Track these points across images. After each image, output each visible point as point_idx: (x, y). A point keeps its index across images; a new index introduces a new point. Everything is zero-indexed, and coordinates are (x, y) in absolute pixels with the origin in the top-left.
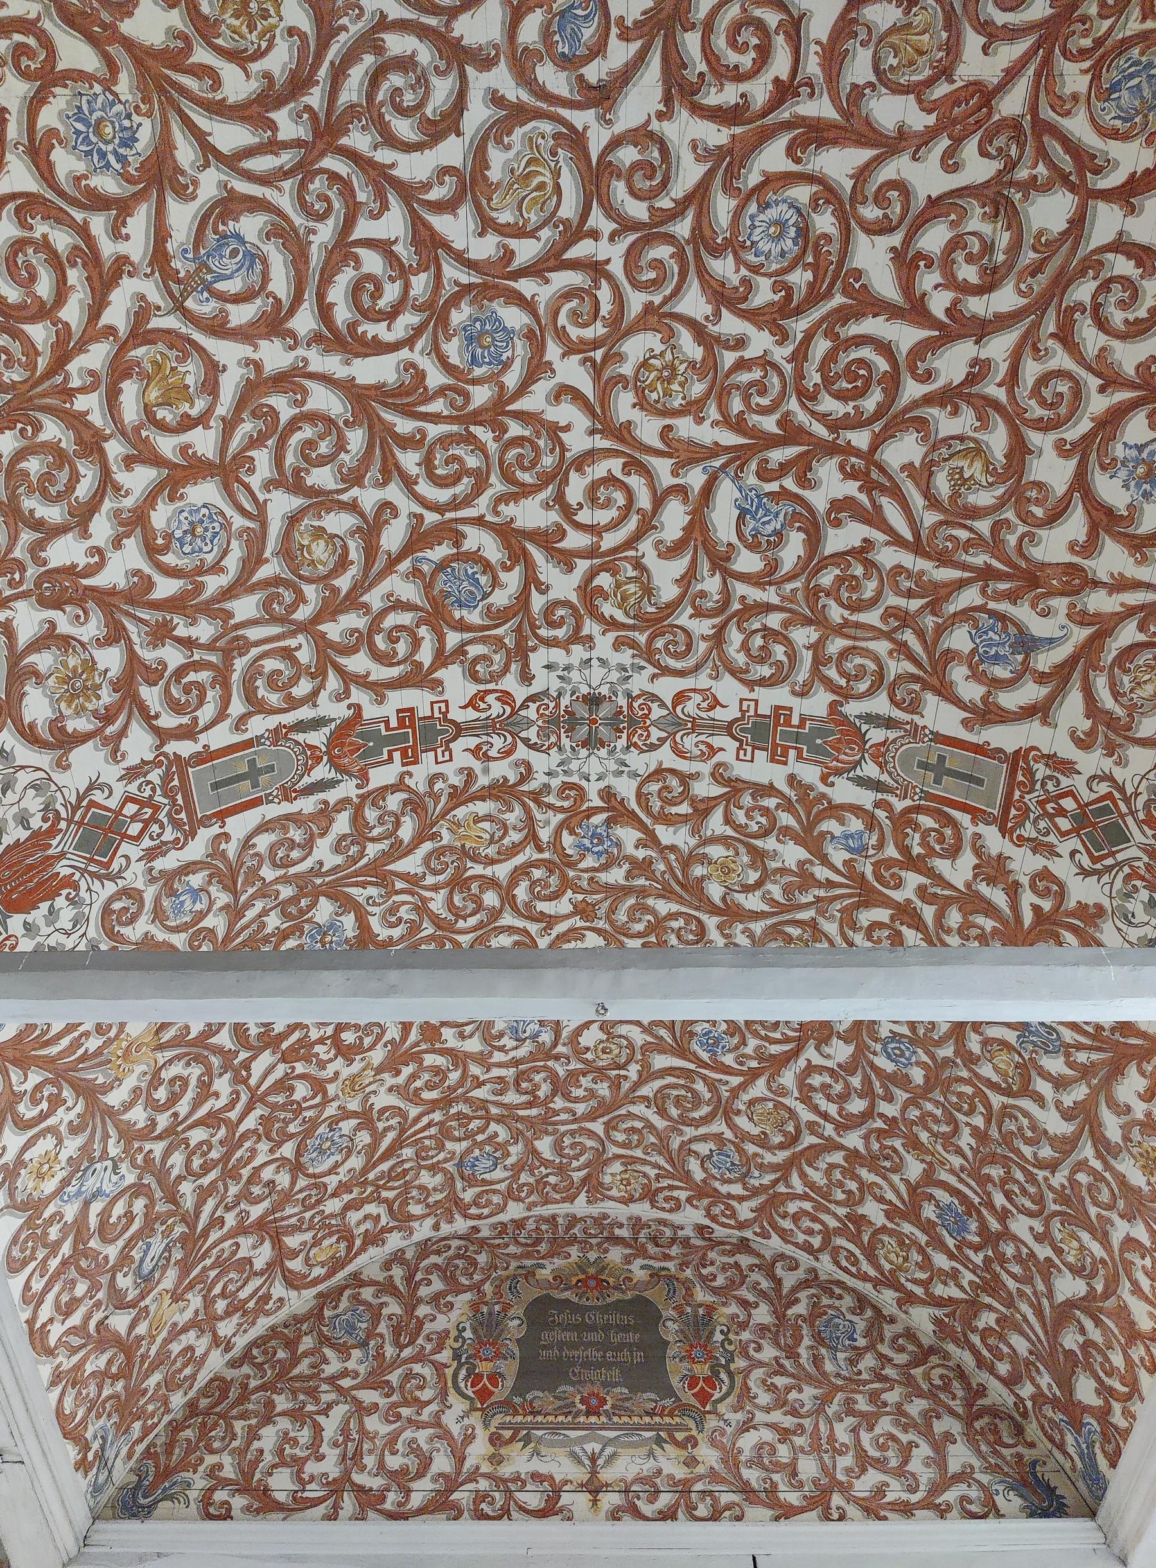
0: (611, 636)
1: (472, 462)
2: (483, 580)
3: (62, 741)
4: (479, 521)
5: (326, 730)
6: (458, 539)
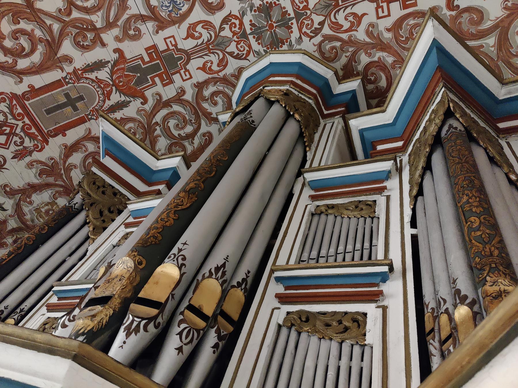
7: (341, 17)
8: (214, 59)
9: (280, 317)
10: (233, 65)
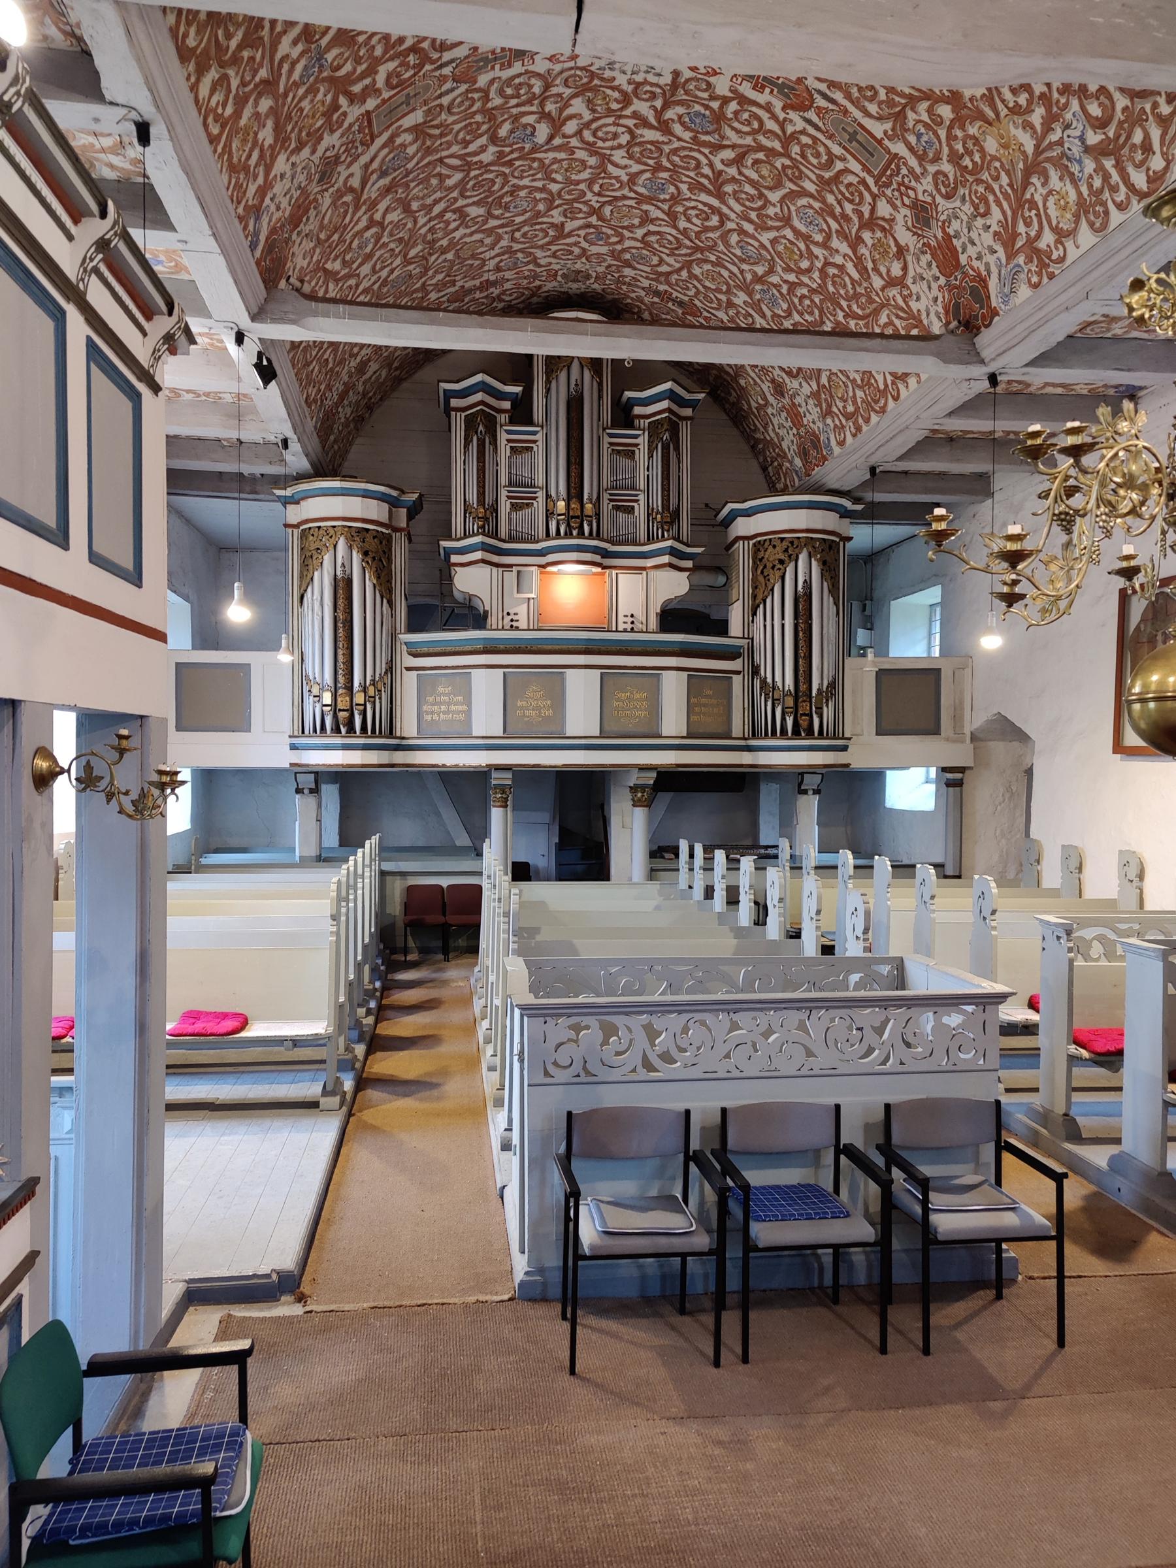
0: (616, 83)
1: (676, 159)
2: (687, 120)
3: (901, 252)
4: (679, 139)
5: (806, 115)
6: (694, 138)
7: (624, 287)
8: (526, 281)
9: (610, 507)
10: (538, 283)
